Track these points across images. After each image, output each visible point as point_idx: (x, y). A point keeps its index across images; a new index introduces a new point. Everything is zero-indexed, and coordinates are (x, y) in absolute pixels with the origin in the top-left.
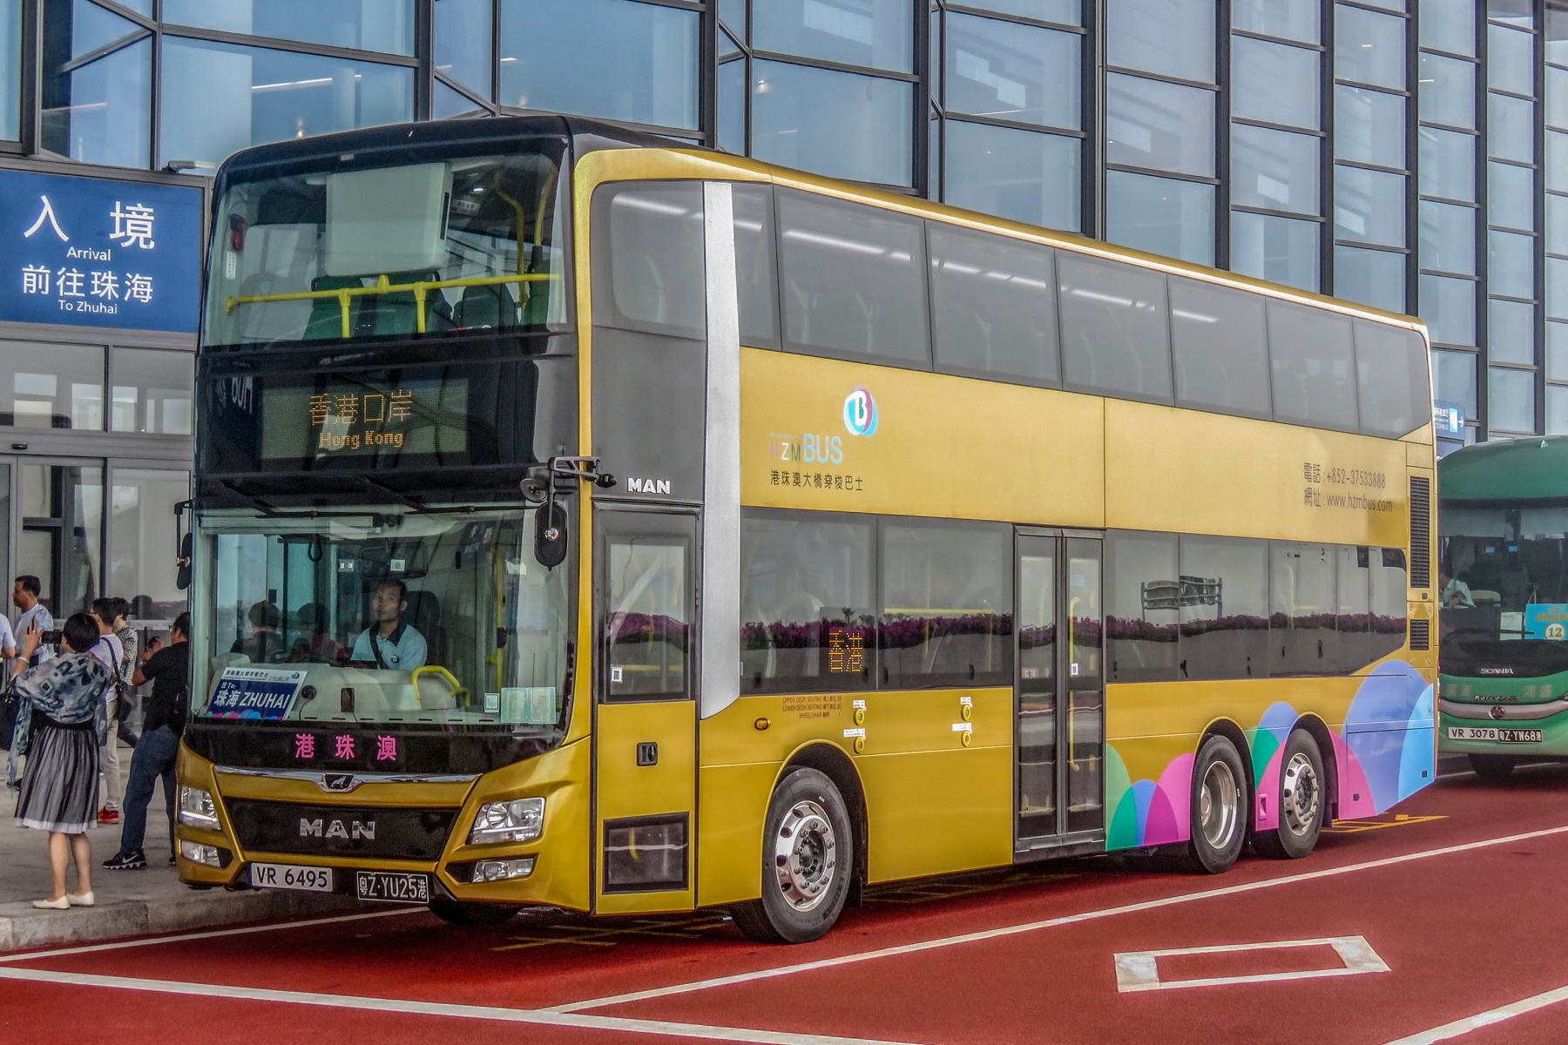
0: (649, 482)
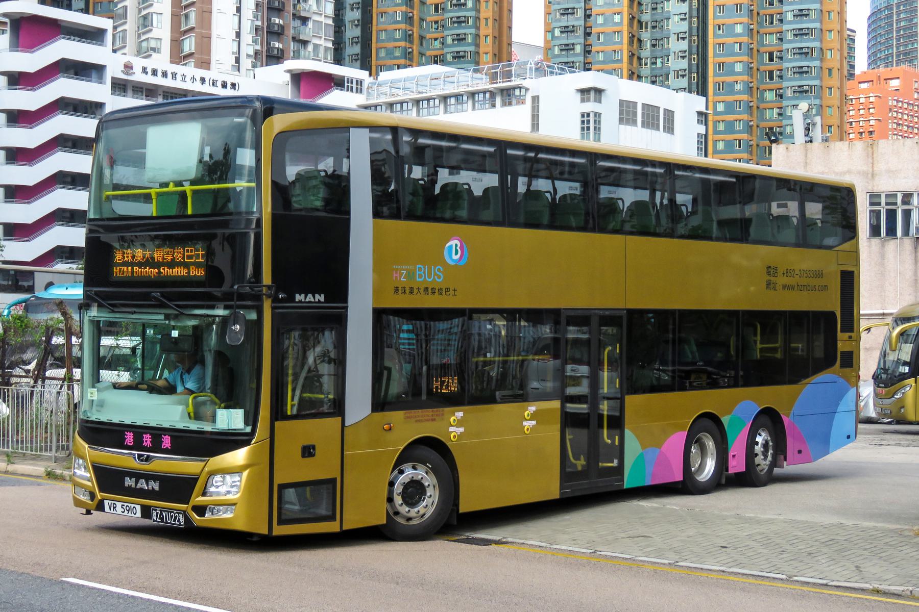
0: (310, 296)
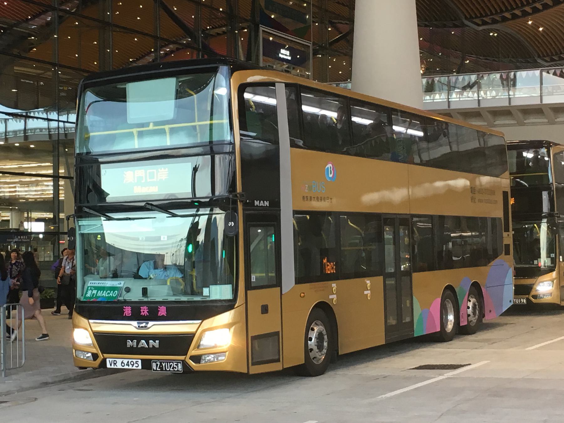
0: (262, 202)
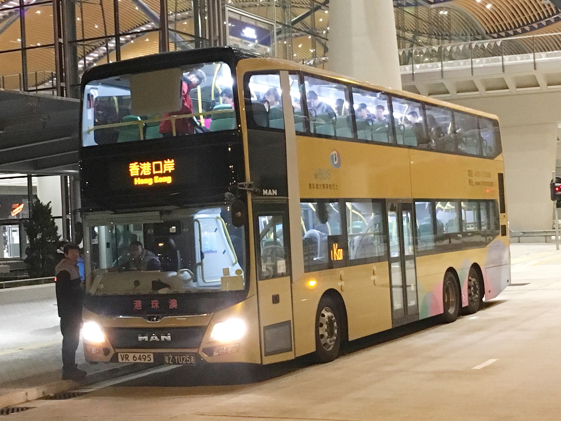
0: (270, 190)
